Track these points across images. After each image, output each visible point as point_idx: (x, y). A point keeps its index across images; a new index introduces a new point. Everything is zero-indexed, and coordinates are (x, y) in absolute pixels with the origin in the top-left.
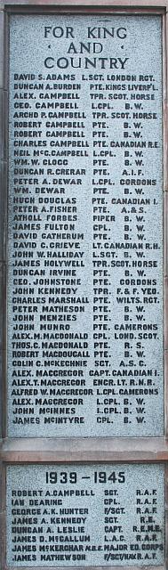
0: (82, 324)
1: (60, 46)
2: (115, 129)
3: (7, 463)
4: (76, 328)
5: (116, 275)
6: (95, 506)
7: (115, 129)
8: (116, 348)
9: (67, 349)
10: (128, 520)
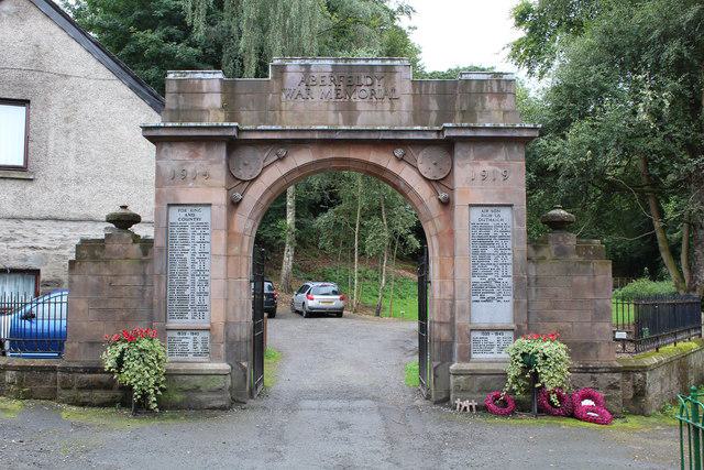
0: (188, 292)
2: (197, 238)
5: (197, 279)
7: (197, 238)
8: (197, 298)
9: (184, 299)
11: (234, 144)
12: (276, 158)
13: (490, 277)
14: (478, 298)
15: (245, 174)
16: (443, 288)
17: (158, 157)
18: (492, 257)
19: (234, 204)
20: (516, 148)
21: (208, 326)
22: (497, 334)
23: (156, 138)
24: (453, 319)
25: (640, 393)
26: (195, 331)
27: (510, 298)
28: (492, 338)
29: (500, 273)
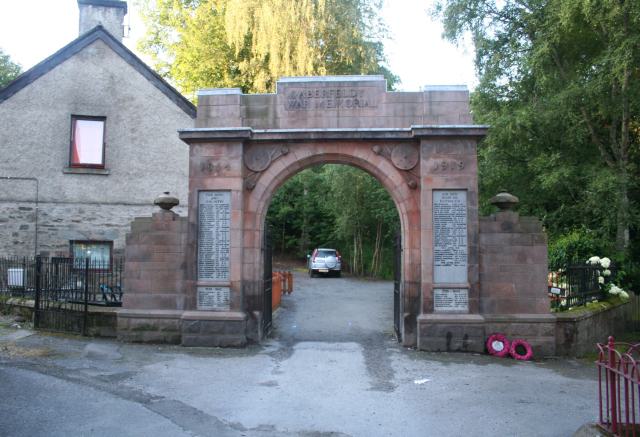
0: (213, 257)
1: (209, 198)
2: (221, 216)
3: (197, 286)
5: (220, 247)
6: (215, 294)
8: (220, 263)
9: (210, 263)
10: (222, 298)
11: (247, 142)
14: (439, 263)
16: (411, 255)
17: (191, 154)
19: (248, 189)
20: (469, 145)
21: (228, 283)
23: (190, 139)
25: (570, 339)
26: (218, 287)
27: (466, 263)
28: (451, 294)
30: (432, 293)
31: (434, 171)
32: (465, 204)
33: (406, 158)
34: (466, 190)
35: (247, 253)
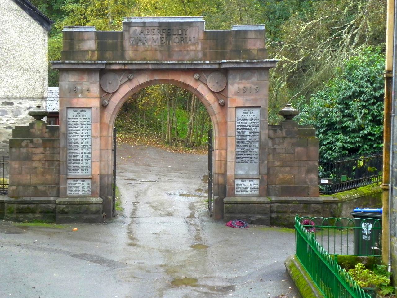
0: (79, 157)
1: (75, 113)
2: (84, 127)
4: (78, 158)
5: (84, 150)
8: (84, 161)
9: (77, 161)
10: (86, 187)
12: (127, 79)
13: (246, 148)
14: (239, 160)
15: (109, 89)
16: (220, 155)
18: (248, 137)
19: (103, 107)
21: (90, 177)
22: (250, 181)
24: (226, 171)
29: (252, 147)
30: (234, 182)
31: (237, 93)
32: (258, 117)
33: (217, 83)
34: (260, 107)
35: (103, 152)
